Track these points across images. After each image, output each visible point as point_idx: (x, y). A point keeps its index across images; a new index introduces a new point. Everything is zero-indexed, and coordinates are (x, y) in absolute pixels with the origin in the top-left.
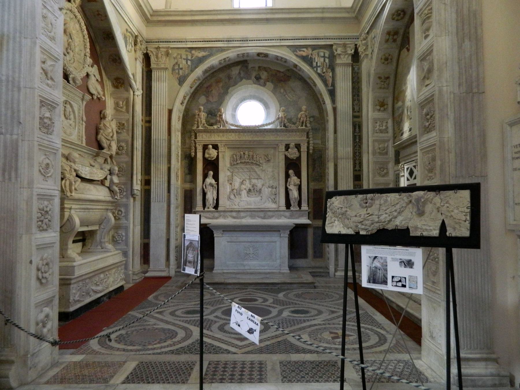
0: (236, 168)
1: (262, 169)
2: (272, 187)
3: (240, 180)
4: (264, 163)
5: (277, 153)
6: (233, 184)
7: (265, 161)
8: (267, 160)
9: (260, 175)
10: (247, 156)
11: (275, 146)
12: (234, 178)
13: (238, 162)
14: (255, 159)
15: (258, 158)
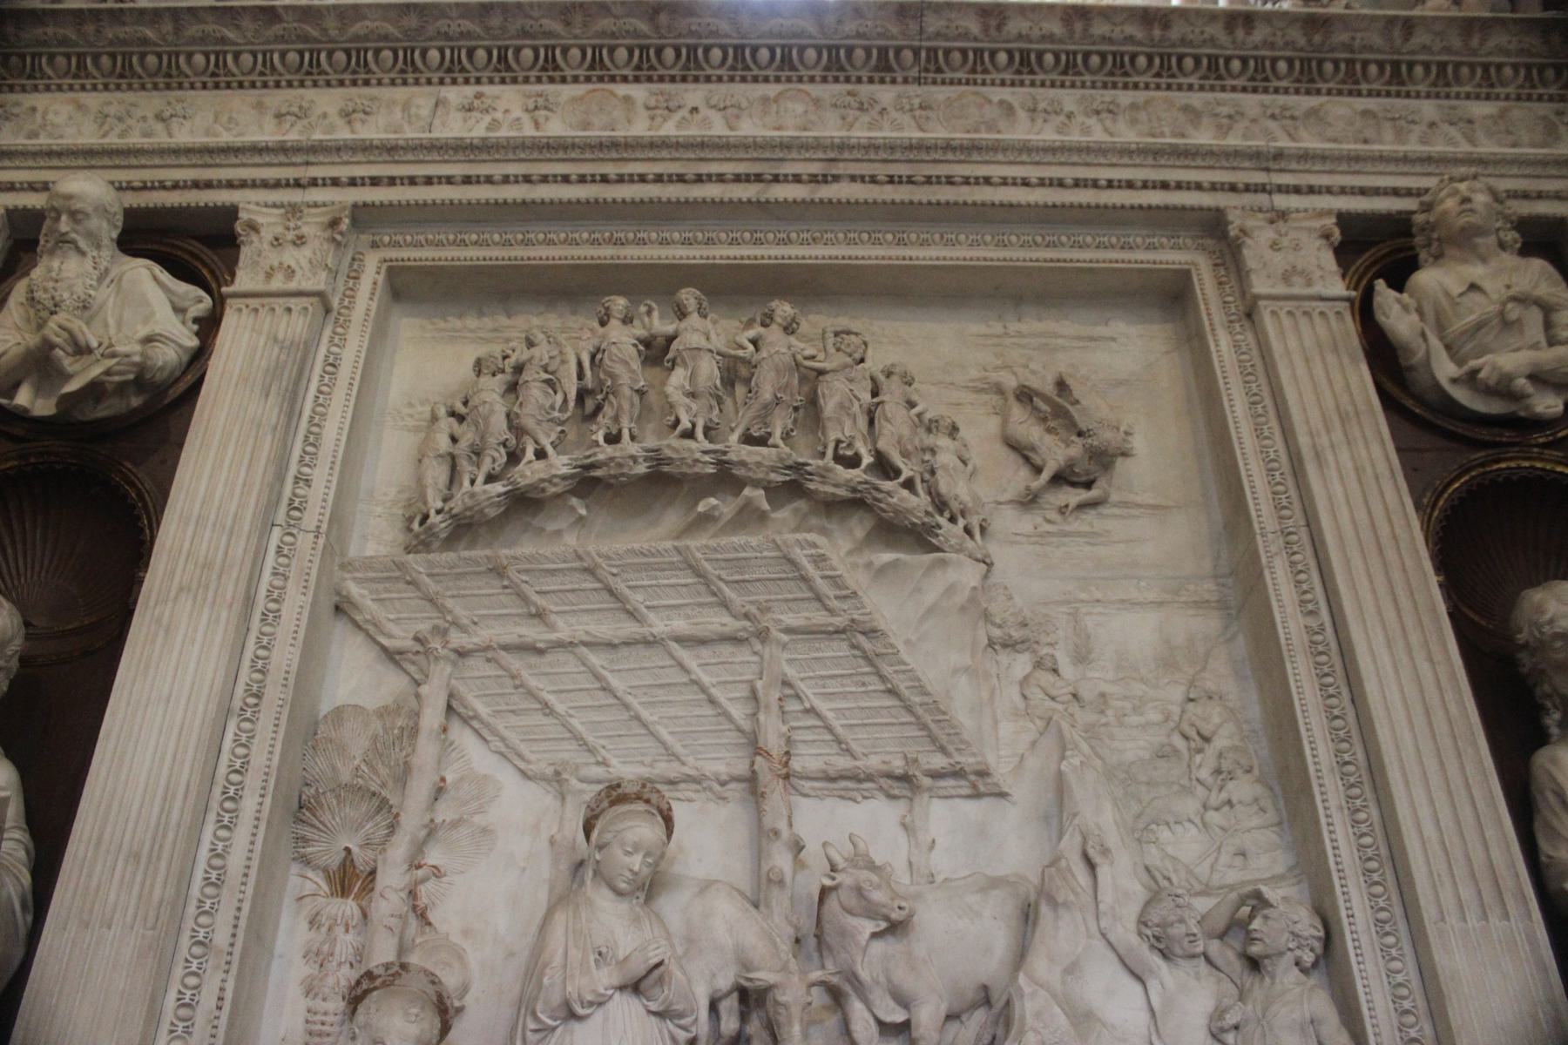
0: (498, 571)
1: (976, 608)
2: (1236, 927)
3: (538, 798)
4: (1008, 521)
5: (1223, 346)
6: (392, 878)
7: (1019, 479)
8: (1056, 452)
9: (963, 718)
10: (709, 371)
11: (1171, 257)
12: (426, 750)
13: (529, 472)
14: (845, 428)
15: (895, 430)
